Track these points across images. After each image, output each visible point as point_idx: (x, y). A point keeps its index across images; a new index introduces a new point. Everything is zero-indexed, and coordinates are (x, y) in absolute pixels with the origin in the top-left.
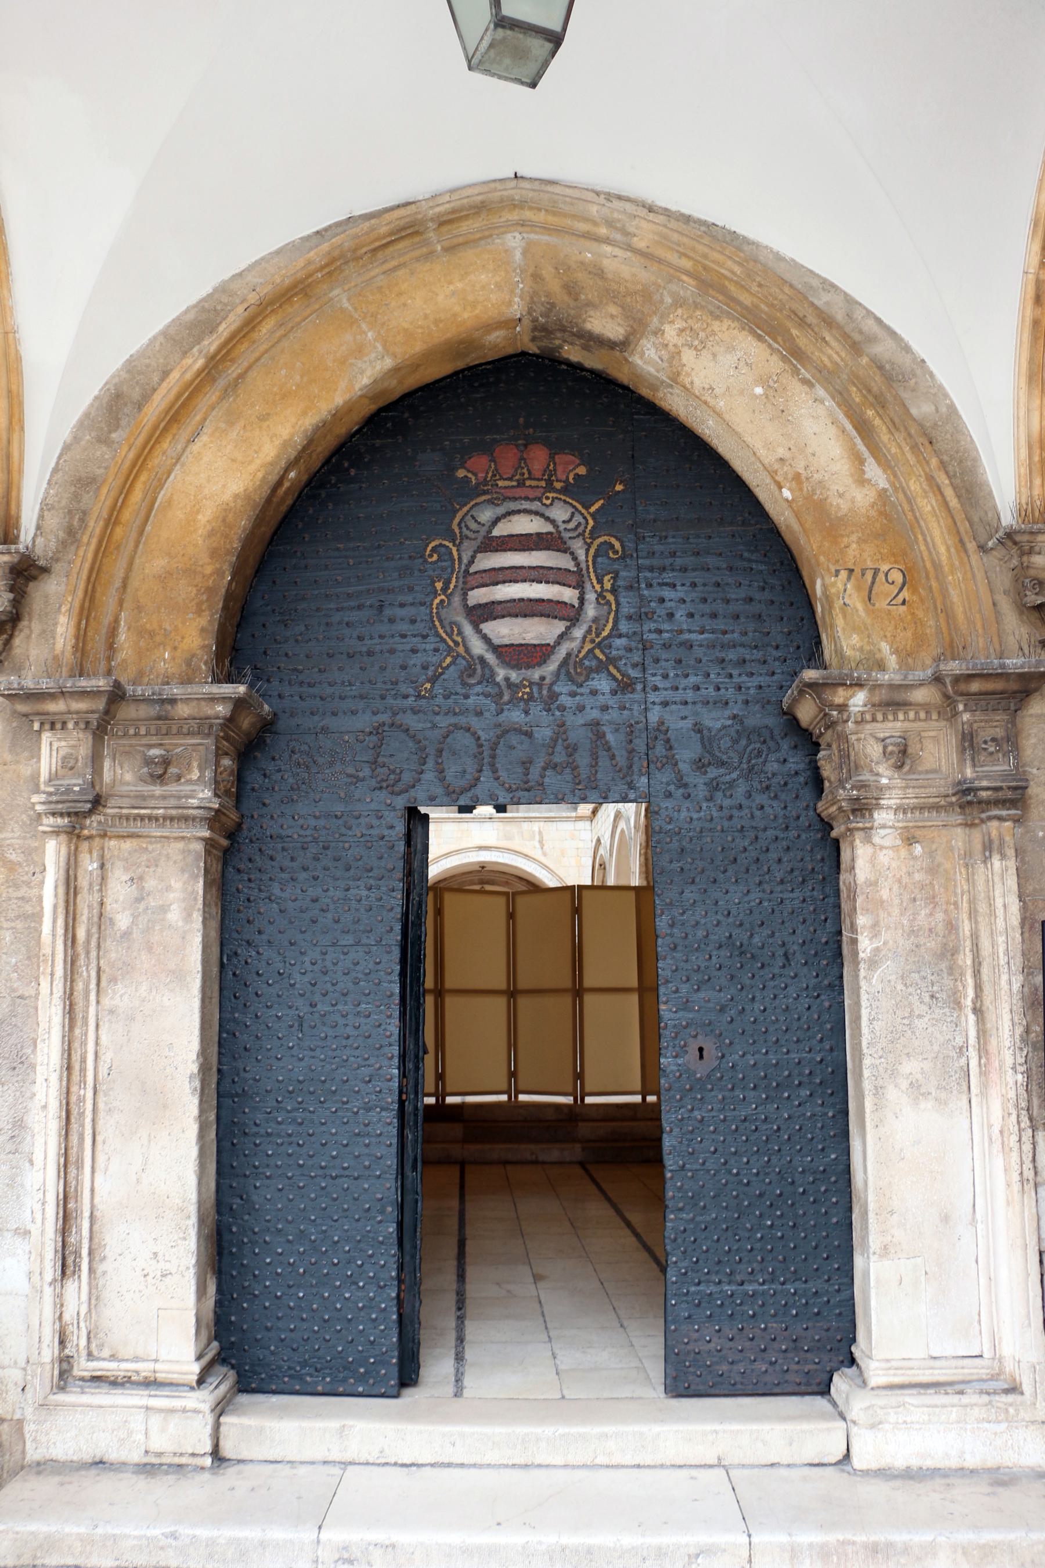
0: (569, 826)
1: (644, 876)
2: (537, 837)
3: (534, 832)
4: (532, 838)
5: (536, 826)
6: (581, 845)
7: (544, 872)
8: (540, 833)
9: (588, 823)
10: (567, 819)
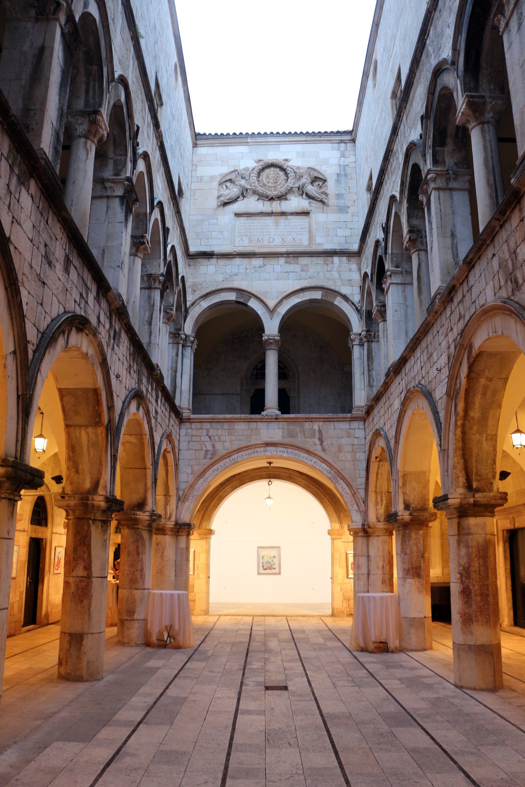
0: (345, 426)
1: (460, 453)
2: (317, 435)
3: (314, 430)
4: (313, 436)
5: (316, 426)
6: (356, 442)
7: (323, 465)
8: (320, 431)
9: (361, 423)
10: (343, 420)
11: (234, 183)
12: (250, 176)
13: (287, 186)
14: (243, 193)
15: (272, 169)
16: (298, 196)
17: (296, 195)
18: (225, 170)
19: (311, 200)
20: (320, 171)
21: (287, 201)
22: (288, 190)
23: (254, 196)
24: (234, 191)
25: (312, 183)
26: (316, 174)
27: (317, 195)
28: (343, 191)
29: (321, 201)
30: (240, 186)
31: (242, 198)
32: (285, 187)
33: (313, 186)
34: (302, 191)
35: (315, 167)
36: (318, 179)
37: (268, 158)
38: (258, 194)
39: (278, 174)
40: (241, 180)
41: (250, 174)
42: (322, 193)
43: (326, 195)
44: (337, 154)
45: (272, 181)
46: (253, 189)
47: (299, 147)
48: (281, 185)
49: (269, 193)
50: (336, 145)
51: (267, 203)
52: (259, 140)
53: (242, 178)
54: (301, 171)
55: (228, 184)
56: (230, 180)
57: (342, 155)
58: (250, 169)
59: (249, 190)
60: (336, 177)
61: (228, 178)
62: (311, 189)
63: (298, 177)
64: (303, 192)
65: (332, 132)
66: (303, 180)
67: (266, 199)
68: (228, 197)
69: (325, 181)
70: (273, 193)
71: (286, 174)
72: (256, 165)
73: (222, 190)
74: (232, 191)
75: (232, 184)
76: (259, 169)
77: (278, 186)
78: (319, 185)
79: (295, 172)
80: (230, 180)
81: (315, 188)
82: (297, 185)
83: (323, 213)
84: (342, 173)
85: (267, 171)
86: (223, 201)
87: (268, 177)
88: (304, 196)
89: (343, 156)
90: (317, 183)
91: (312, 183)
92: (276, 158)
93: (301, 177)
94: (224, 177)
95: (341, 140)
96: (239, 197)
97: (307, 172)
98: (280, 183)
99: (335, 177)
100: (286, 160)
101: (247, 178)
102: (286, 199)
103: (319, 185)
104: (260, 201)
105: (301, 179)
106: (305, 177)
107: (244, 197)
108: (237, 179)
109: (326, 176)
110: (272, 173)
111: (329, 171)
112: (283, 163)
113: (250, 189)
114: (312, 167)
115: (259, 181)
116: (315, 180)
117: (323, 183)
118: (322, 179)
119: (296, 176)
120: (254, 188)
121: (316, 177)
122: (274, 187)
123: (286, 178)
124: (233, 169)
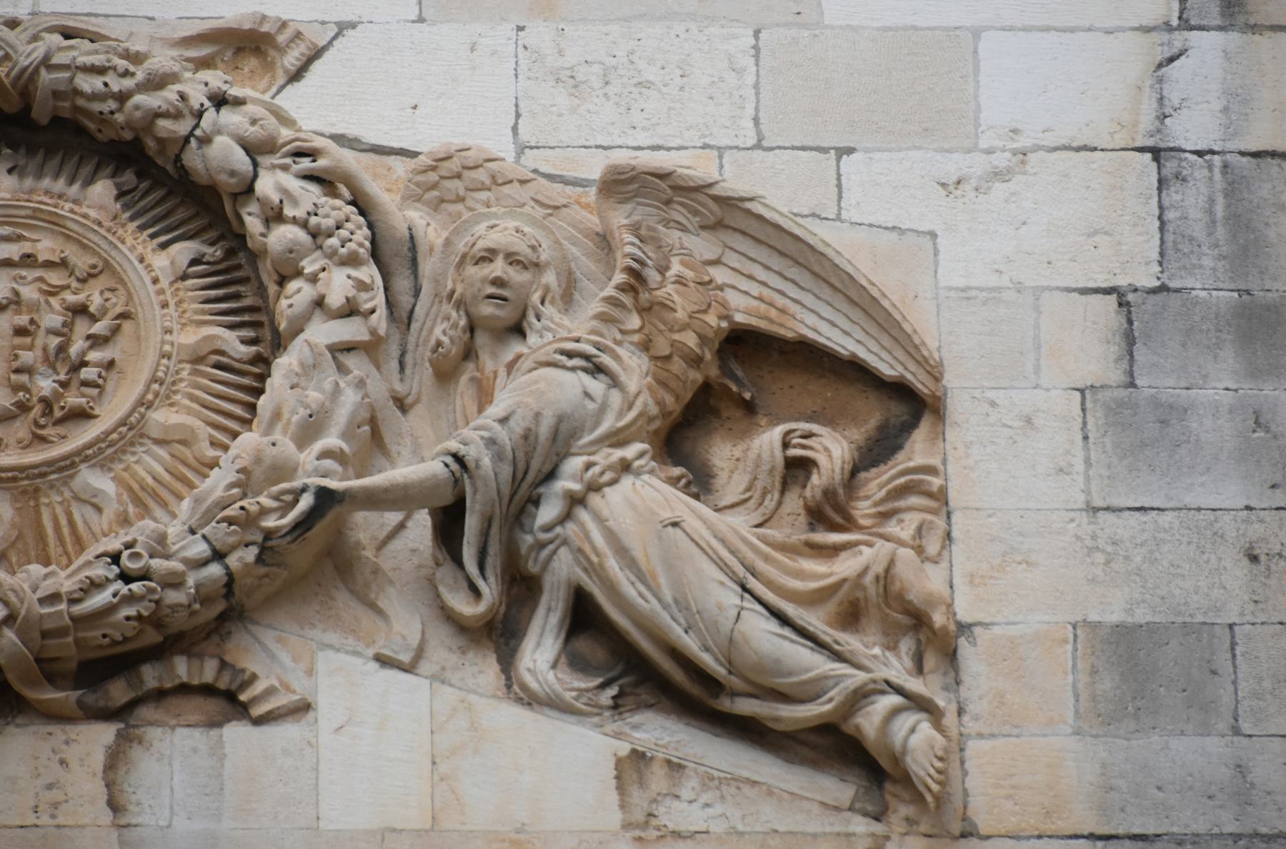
13: (245, 483)
16: (443, 650)
17: (406, 623)
19: (658, 731)
20: (824, 235)
21: (236, 732)
22: (268, 548)
25: (680, 437)
27: (761, 634)
29: (836, 746)
32: (217, 483)
33: (700, 483)
35: (734, 182)
39: (102, 269)
42: (851, 617)
43: (929, 635)
48: (149, 463)
54: (501, 229)
63: (439, 328)
66: (531, 389)
69: (907, 407)
71: (239, 277)
78: (798, 468)
81: (740, 523)
82: (415, 464)
88: (540, 652)
90: (768, 441)
93: (501, 322)
97: (604, 242)
98: (131, 432)
99: (1085, 344)
100: (247, 44)
102: (229, 701)
103: (797, 468)
105: (491, 361)
106: (556, 327)
109: (936, 327)
112: (196, 87)
117: (879, 449)
118: (855, 372)
119: (401, 318)
121: (743, 344)
123: (234, 344)
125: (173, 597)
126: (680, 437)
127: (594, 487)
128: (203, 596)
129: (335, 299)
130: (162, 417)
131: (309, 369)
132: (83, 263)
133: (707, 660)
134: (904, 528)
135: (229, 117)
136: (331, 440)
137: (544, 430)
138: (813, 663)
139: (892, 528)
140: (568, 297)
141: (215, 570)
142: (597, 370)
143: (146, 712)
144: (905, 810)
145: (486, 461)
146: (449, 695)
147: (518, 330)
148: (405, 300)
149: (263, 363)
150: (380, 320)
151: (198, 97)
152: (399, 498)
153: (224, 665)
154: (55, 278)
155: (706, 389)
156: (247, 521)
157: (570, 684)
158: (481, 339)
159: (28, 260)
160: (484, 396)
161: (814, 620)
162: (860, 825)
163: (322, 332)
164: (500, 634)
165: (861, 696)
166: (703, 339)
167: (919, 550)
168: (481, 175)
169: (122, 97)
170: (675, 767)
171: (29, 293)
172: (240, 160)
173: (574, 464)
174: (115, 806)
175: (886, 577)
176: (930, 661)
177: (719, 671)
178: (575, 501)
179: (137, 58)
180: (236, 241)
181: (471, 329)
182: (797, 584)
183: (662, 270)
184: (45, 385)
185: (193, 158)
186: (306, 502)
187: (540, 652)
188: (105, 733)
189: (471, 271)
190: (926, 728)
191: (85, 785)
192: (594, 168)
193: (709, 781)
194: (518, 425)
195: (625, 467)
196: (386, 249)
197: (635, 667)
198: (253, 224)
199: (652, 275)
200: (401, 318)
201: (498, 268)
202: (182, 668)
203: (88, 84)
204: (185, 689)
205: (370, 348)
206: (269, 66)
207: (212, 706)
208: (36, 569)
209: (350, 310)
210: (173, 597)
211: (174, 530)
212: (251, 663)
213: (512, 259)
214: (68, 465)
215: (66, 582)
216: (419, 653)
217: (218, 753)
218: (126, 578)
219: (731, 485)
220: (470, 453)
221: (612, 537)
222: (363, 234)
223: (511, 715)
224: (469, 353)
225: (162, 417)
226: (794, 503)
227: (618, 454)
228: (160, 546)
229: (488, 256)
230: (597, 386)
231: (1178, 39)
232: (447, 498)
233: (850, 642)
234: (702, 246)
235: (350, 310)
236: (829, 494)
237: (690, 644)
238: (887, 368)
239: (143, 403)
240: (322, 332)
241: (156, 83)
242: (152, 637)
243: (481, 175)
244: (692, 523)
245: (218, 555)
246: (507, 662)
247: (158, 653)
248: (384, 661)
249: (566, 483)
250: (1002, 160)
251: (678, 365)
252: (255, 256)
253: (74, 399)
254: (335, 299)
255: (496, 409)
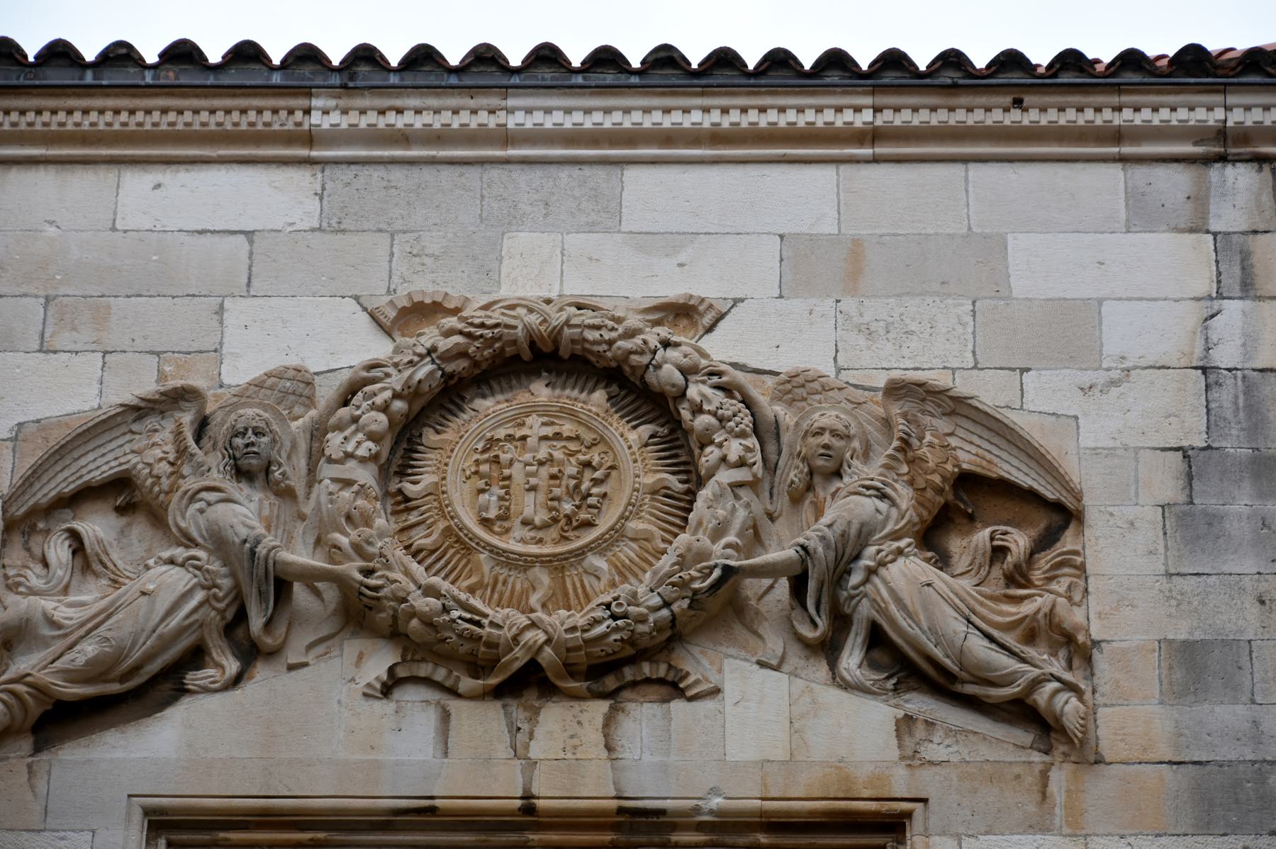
11: (158, 518)
12: (316, 456)
13: (682, 563)
14: (241, 616)
15: (541, 391)
16: (795, 659)
17: (774, 643)
18: (74, 389)
19: (919, 704)
20: (1016, 419)
21: (678, 706)
23: (353, 647)
24: (155, 588)
26: (971, 452)
27: (978, 647)
28: (1243, 619)
30: (219, 542)
31: (232, 666)
33: (943, 561)
34: (830, 612)
35: (962, 386)
36: (994, 500)
37: (506, 292)
38: (395, 634)
40: (231, 487)
41: (318, 432)
42: (1030, 637)
43: (1077, 649)
44: (1184, 263)
45: (530, 506)
46: (340, 581)
47: (806, 196)
48: (627, 552)
49: (504, 619)
50: (1173, 183)
51: (482, 723)
52: (419, 114)
53: (241, 473)
54: (827, 416)
55: (97, 526)
56: (121, 493)
57: (1233, 273)
58: (327, 391)
59: (298, 589)
60: (1167, 486)
61: (98, 465)
62: (921, 592)
63: (793, 473)
64: (841, 622)
65: (1131, 60)
66: (845, 508)
67: (467, 683)
68: (89, 649)
69: (1061, 516)
70: (536, 620)
72: (381, 348)
73: (34, 578)
74: (130, 588)
75: (140, 529)
76: (411, 393)
77: (600, 563)
78: (999, 552)
79: (765, 431)
80: (121, 493)
81: (966, 584)
82: (779, 552)
83: (1045, 829)
84: (1234, 445)
85: (489, 410)
86: (40, 690)
87: (491, 468)
88: (852, 660)
89: (1240, 275)
90: (982, 536)
91: (932, 535)
92: (577, 287)
94: (62, 452)
95: (1221, 134)
96: (196, 656)
97: (887, 423)
99: (1164, 482)
100: (681, 312)
101: (293, 470)
102: (674, 688)
103: (999, 552)
104: (411, 695)
107: (252, 654)
108: (191, 483)
110: (535, 426)
111: (1107, 431)
112: (652, 337)
113: (310, 577)
114: (940, 379)
115: (403, 503)
116: (957, 504)
117: (1045, 541)
118: (1031, 496)
119: (771, 468)
120: (352, 569)
121: (968, 482)
122: (556, 564)
123: (674, 483)
124: (147, 386)
125: (641, 628)
126: (932, 535)
127: (882, 564)
128: (658, 628)
129: (733, 457)
130: (634, 525)
131: (718, 497)
132: (588, 437)
133: (948, 662)
134: (1060, 586)
135: (672, 354)
136: (731, 538)
137: (853, 531)
138: (1007, 663)
139: (1054, 586)
140: (866, 455)
141: (665, 612)
142: (883, 496)
143: (626, 694)
144: (1062, 748)
145: (820, 549)
146: (799, 683)
147: (838, 474)
148: (773, 457)
149: (692, 494)
150: (758, 469)
151: (653, 342)
152: (770, 571)
153: (670, 667)
154: (573, 446)
155: (946, 508)
156: (683, 584)
157: (869, 677)
158: (817, 480)
159: (557, 436)
160: (819, 512)
161: (1009, 639)
162: (1037, 757)
163: (725, 476)
164: (828, 649)
165: (1036, 683)
166: (944, 478)
167: (1070, 599)
168: (816, 385)
169: (610, 343)
170: (930, 724)
171: (558, 455)
172: (678, 377)
173: (871, 550)
174: (609, 748)
175: (1051, 614)
176: (1076, 662)
177: (954, 668)
178: (871, 572)
179: (619, 320)
180: (675, 423)
181: (811, 473)
182: (999, 619)
183: (921, 439)
184: (567, 507)
185: (651, 377)
186: (717, 573)
187: (852, 660)
188: (603, 706)
189: (811, 440)
190: (1074, 701)
191: (592, 735)
192: (881, 381)
193: (949, 732)
194: (838, 528)
195: (900, 552)
196: (762, 428)
197: (908, 668)
198: (686, 414)
199: (915, 442)
200: (771, 468)
201: (826, 438)
202: (646, 669)
203: (592, 335)
204: (648, 681)
205: (753, 485)
206: (694, 324)
207: (664, 690)
208: (563, 613)
209: (741, 463)
210: (641, 628)
211: (641, 590)
212: (686, 666)
213: (834, 433)
214: (581, 553)
215: (580, 620)
216: (783, 659)
217: (668, 717)
218: (614, 617)
219: (961, 562)
220: (811, 544)
221: (892, 592)
222: (748, 420)
223: (834, 695)
224: (810, 487)
225: (634, 525)
226: (997, 572)
227: (896, 544)
228: (633, 599)
229: (820, 432)
230: (883, 506)
231: (1216, 305)
232: (797, 570)
233: (1030, 652)
234: (943, 425)
235: (741, 463)
236: (1017, 567)
237: (938, 653)
238: (1050, 495)
239: (623, 517)
240: (725, 476)
241: (630, 334)
242: (630, 651)
243: (816, 385)
244: (938, 584)
245: (667, 604)
246: (833, 665)
247: (633, 660)
248: (762, 664)
249: (866, 562)
250: (1115, 374)
251: (930, 493)
252: (687, 433)
253: (584, 516)
254: (733, 457)
255: (825, 520)
